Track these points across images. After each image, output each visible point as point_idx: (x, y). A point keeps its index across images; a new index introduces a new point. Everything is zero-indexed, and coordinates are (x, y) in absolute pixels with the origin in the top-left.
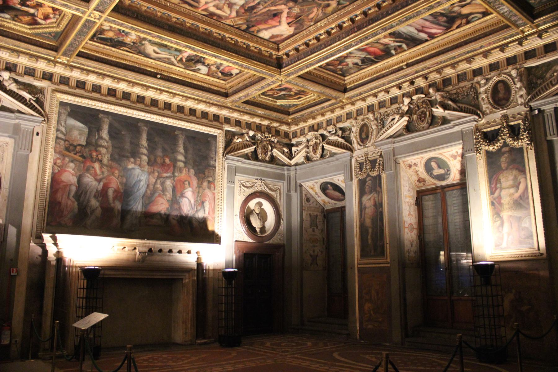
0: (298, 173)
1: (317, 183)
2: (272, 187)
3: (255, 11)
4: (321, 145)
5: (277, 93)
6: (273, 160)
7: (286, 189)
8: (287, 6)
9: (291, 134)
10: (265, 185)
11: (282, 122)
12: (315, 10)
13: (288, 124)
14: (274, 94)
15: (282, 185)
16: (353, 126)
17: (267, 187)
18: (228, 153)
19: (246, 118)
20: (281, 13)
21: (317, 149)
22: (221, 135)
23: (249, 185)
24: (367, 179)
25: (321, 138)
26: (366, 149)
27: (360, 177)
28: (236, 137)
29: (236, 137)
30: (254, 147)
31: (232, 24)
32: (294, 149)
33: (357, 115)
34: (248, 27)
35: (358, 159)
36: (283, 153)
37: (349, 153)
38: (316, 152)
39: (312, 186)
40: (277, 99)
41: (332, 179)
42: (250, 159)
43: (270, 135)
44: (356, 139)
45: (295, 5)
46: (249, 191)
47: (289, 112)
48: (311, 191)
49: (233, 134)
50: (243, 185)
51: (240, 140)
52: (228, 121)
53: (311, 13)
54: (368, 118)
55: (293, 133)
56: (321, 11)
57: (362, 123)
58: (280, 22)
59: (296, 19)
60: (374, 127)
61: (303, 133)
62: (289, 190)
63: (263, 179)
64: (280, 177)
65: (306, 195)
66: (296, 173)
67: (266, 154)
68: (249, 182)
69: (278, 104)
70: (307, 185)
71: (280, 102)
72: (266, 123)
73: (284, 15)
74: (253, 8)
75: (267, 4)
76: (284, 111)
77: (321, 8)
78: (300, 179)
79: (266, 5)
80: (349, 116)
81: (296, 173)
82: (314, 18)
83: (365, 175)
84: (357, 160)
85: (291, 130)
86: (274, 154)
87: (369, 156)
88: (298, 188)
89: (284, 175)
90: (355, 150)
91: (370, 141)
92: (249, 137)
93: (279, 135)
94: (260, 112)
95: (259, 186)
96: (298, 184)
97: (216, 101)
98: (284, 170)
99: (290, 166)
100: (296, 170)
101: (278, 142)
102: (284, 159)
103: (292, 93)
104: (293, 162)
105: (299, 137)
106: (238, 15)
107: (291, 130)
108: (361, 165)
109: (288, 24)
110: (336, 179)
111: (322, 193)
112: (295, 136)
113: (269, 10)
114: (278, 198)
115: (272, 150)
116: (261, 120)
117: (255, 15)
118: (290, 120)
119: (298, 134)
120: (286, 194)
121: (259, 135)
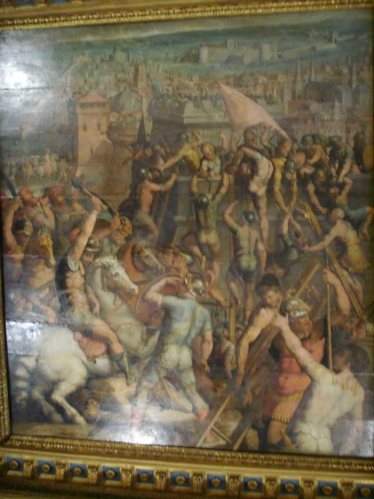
3: (229, 367)
8: (270, 306)
12: (331, 278)
20: (280, 337)
31: (222, 442)
34: (263, 434)
45: (284, 293)
53: (335, 295)
56: (345, 273)
58: (303, 370)
59: (325, 335)
73: (292, 340)
74: (218, 359)
75: (232, 326)
77: (336, 265)
79: (232, 334)
82: (358, 309)
106: (213, 406)
109: (324, 362)
113: (251, 345)
117: (239, 380)
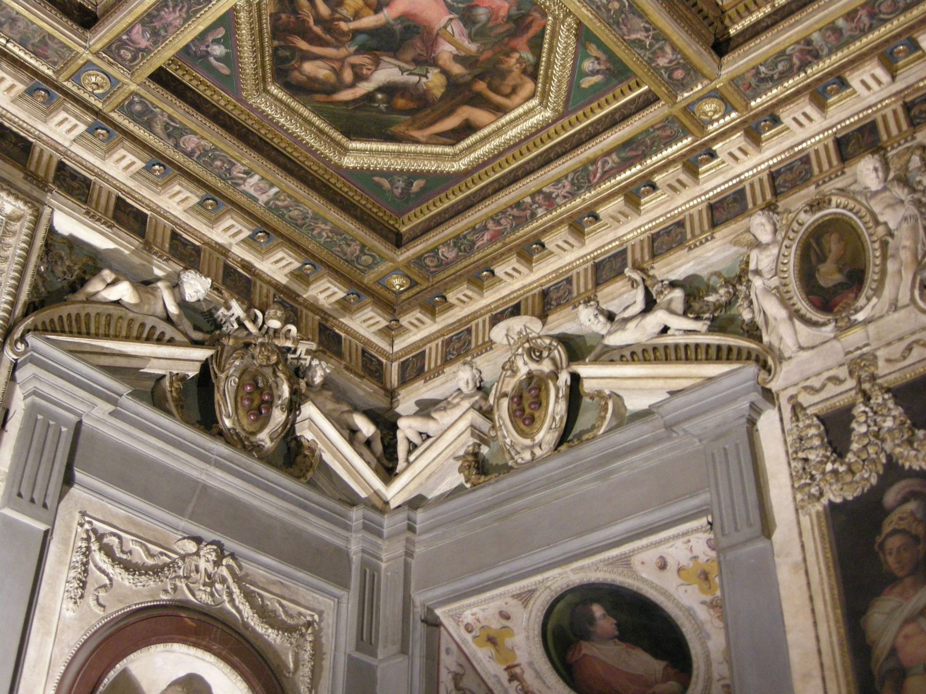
0: (418, 550)
1: (525, 597)
2: (272, 602)
4: (564, 377)
5: (359, 77)
6: (293, 455)
7: (348, 638)
9: (395, 365)
10: (238, 580)
11: (361, 292)
13: (391, 306)
14: (334, 89)
15: (330, 610)
16: (757, 244)
17: (249, 596)
18: (42, 330)
19: (175, 203)
21: (539, 403)
22: (16, 226)
23: (140, 555)
24: (891, 497)
25: (560, 353)
26: (854, 337)
27: (834, 495)
28: (108, 275)
29: (108, 275)
30: (202, 354)
32: (407, 428)
33: (775, 193)
35: (805, 399)
36: (351, 434)
37: (751, 369)
38: (532, 419)
39: (496, 624)
40: (351, 134)
41: (625, 561)
42: (168, 412)
43: (293, 329)
44: (784, 302)
46: (135, 591)
47: (399, 235)
48: (482, 655)
49: (93, 262)
50: (108, 551)
51: (124, 292)
52: (75, 185)
54: (842, 191)
55: (404, 366)
57: (809, 219)
60: (891, 218)
61: (460, 345)
62: (366, 639)
63: (230, 544)
64: (327, 564)
65: (457, 678)
66: (409, 554)
67: (260, 411)
68: (143, 540)
69: (349, 162)
70: (468, 617)
71: (362, 154)
72: (276, 266)
76: (380, 209)
78: (427, 584)
80: (725, 209)
81: (409, 554)
83: (869, 477)
84: (797, 408)
85: (401, 344)
86: (306, 434)
87: (882, 368)
88: (419, 631)
89: (343, 555)
90: (781, 359)
91: (878, 292)
92: (182, 304)
93: (339, 354)
94: (259, 184)
95: (200, 577)
96: (418, 612)
97: (23, 43)
98: (347, 528)
99: (381, 506)
100: (411, 528)
101: (327, 383)
102: (354, 468)
103: (434, 81)
104: (396, 492)
105: (438, 372)
107: (401, 344)
108: (836, 428)
110: (651, 556)
111: (545, 667)
112: (415, 368)
114: (305, 670)
115: (293, 407)
116: (250, 243)
118: (397, 282)
119: (432, 361)
120: (350, 659)
121: (237, 310)
